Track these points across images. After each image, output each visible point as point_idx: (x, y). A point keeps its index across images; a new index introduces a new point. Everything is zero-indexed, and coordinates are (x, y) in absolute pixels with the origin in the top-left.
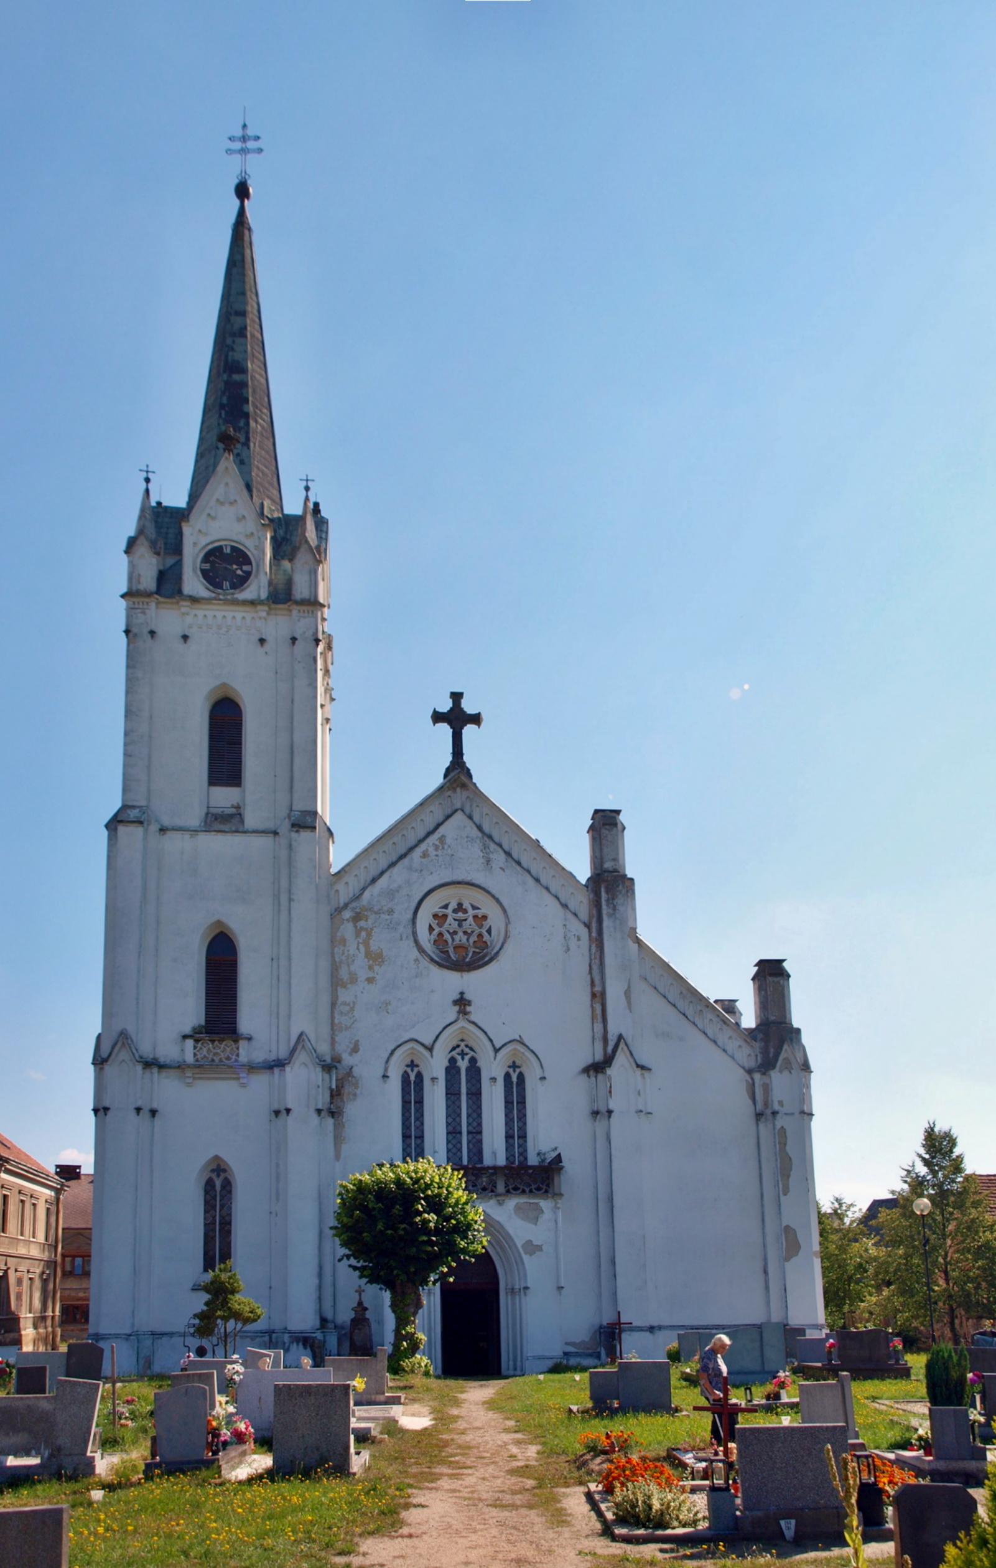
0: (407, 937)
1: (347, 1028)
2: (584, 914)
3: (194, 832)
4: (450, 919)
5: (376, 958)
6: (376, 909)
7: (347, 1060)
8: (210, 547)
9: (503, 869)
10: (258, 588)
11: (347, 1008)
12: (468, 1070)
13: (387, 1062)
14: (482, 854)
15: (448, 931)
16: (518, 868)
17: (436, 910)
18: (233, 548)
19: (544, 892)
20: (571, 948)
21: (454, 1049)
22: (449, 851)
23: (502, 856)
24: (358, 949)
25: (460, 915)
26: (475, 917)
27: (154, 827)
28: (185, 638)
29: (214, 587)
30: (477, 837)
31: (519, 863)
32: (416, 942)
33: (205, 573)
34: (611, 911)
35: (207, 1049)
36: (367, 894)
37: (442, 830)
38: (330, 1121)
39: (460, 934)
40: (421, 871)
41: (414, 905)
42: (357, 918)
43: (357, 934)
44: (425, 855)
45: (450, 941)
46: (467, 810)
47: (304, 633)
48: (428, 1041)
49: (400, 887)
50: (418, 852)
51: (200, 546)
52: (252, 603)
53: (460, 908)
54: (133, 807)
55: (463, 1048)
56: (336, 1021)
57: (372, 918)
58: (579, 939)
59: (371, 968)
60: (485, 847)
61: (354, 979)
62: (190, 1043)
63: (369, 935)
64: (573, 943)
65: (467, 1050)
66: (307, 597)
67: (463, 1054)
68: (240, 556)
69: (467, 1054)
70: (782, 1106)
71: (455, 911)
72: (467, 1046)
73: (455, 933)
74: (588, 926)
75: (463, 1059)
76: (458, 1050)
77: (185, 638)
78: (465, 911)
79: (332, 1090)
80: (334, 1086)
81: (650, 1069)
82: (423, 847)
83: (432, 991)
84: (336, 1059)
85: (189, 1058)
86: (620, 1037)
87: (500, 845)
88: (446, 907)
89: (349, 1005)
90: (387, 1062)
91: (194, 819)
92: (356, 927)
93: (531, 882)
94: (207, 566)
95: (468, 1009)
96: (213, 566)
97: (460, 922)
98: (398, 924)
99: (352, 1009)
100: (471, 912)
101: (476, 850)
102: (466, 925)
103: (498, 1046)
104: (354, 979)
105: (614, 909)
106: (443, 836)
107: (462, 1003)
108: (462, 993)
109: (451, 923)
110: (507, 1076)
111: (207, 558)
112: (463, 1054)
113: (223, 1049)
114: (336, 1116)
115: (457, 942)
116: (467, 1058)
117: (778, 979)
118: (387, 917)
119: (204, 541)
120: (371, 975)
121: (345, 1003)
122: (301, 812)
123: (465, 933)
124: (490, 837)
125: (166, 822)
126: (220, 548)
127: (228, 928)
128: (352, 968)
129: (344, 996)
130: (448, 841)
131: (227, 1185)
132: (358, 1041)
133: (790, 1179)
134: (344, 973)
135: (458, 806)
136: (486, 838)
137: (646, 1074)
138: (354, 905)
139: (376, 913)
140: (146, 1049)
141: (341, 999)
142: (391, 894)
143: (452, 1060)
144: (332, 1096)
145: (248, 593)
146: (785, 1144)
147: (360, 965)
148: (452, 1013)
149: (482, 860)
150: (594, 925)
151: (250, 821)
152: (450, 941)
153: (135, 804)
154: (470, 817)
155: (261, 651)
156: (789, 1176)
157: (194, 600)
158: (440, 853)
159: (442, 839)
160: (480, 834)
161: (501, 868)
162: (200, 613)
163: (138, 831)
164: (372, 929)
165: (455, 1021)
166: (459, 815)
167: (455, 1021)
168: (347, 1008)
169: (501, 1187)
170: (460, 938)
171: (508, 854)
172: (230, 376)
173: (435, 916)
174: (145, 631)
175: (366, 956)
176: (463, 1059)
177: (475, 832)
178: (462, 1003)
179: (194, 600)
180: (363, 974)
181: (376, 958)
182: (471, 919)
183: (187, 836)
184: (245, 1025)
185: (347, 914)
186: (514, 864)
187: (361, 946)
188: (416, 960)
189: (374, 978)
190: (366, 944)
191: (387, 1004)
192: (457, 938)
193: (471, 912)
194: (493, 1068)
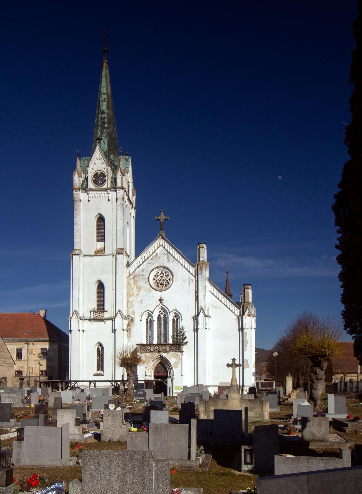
0: (147, 282)
1: (132, 307)
2: (194, 274)
3: (92, 256)
4: (159, 276)
6: (139, 275)
7: (131, 315)
8: (95, 173)
9: (172, 262)
10: (108, 184)
11: (131, 302)
12: (163, 317)
13: (141, 316)
14: (167, 258)
15: (158, 280)
16: (177, 261)
17: (155, 274)
18: (101, 173)
19: (184, 268)
20: (190, 284)
21: (160, 312)
22: (159, 258)
23: (173, 258)
24: (134, 286)
25: (162, 275)
26: (166, 276)
27: (82, 256)
28: (89, 201)
29: (96, 185)
30: (166, 253)
31: (177, 260)
32: (149, 283)
33: (94, 181)
34: (201, 273)
35: (96, 315)
36: (137, 271)
37: (156, 252)
38: (127, 332)
39: (162, 280)
40: (151, 264)
41: (149, 273)
42: (134, 278)
43: (134, 282)
44: (152, 259)
45: (159, 282)
46: (164, 246)
47: (120, 197)
48: (152, 311)
49: (145, 268)
50: (150, 258)
51: (92, 173)
52: (106, 190)
54: (77, 250)
56: (129, 306)
57: (138, 277)
58: (193, 281)
59: (137, 291)
60: (168, 256)
61: (133, 294)
62: (92, 313)
63: (137, 283)
64: (191, 282)
65: (163, 312)
66: (121, 186)
67: (162, 313)
68: (103, 175)
69: (163, 313)
70: (246, 326)
71: (160, 274)
72: (163, 311)
73: (160, 280)
74: (195, 277)
75: (162, 315)
76: (161, 312)
77: (89, 201)
78: (163, 274)
79: (127, 324)
80: (128, 323)
81: (210, 317)
82: (152, 256)
83: (154, 297)
84: (129, 316)
85: (92, 317)
86: (202, 308)
87: (172, 255)
88: (158, 273)
89: (132, 301)
90: (141, 316)
91: (93, 253)
92: (134, 280)
93: (180, 265)
94: (94, 179)
95: (163, 301)
96: (96, 179)
97: (161, 277)
98: (145, 279)
99: (133, 303)
100: (165, 274)
101: (166, 257)
102: (163, 278)
103: (170, 311)
104: (133, 294)
105: (202, 272)
106: (157, 253)
107: (161, 300)
108: (161, 297)
110: (173, 319)
111: (94, 177)
112: (162, 313)
113: (101, 314)
114: (128, 331)
115: (161, 283)
116: (163, 314)
117: (248, 290)
118: (142, 277)
119: (93, 171)
120: (138, 293)
121: (131, 301)
122: (119, 249)
123: (163, 280)
124: (169, 253)
125: (85, 254)
126: (97, 173)
127: (102, 282)
128: (133, 291)
129: (131, 299)
130: (158, 254)
131: (103, 349)
132: (134, 311)
133: (247, 346)
134: (131, 293)
135: (161, 244)
136: (168, 253)
137: (209, 318)
138: (133, 274)
139: (139, 276)
140: (81, 315)
141: (130, 300)
142: (143, 270)
143: (159, 315)
144: (127, 326)
145: (105, 187)
146: (246, 337)
147: (135, 291)
149: (167, 260)
150: (196, 277)
151: (107, 252)
152: (159, 282)
153: (77, 249)
154: (164, 248)
155: (109, 203)
156: (247, 346)
157: (91, 190)
158: (156, 258)
159: (157, 254)
160: (167, 252)
161: (172, 262)
163: (78, 256)
164: (138, 280)
165: (159, 305)
166: (161, 247)
167: (159, 305)
168: (131, 302)
169: (168, 350)
171: (174, 258)
172: (101, 115)
173: (155, 276)
174: (78, 200)
175: (136, 288)
176: (162, 315)
177: (165, 252)
178: (161, 300)
179: (91, 190)
180: (136, 293)
181: (139, 289)
182: (164, 276)
183: (91, 257)
184: (106, 308)
185: (131, 277)
186: (176, 260)
187: (135, 285)
188: (149, 289)
189: (138, 294)
190: (136, 284)
191: (142, 301)
192: (161, 281)
193: (165, 274)
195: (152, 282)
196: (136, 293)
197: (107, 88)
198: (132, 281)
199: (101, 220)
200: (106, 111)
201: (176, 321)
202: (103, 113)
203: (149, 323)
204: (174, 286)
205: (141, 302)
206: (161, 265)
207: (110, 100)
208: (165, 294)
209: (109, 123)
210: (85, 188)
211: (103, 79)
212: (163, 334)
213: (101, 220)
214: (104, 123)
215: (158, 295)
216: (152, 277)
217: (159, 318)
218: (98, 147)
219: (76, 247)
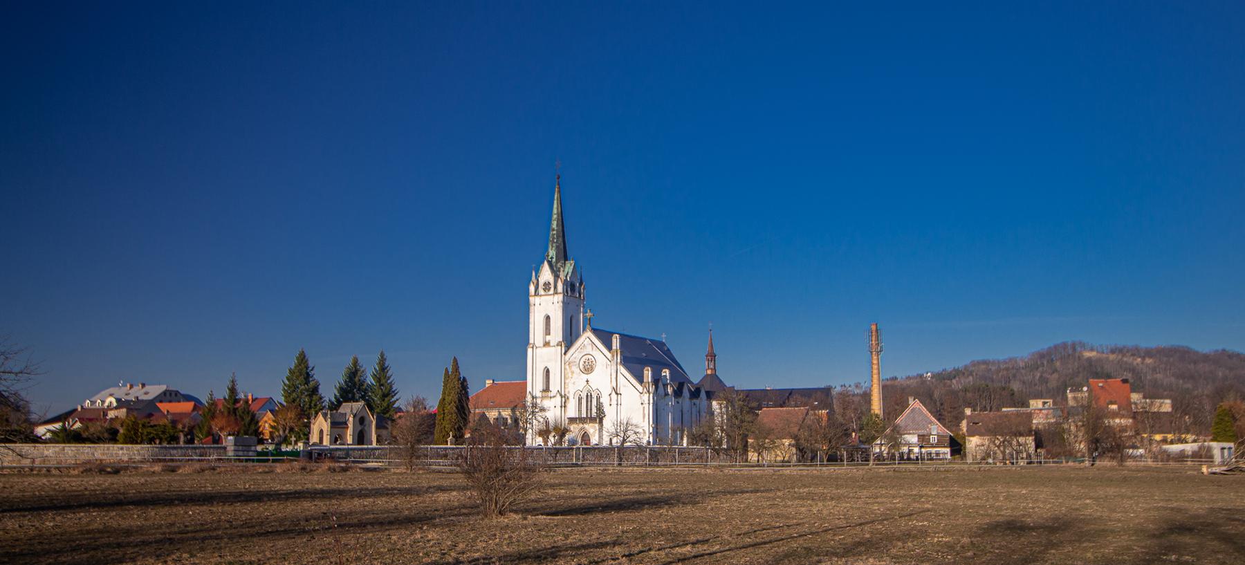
5: (573, 372)
7: (568, 395)
10: (552, 291)
52: (551, 295)
53: (588, 360)
55: (589, 391)
91: (542, 345)
101: (590, 346)
107: (587, 381)
109: (587, 363)
134: (567, 376)
142: (575, 358)
148: (586, 383)
151: (551, 344)
157: (541, 296)
162: (543, 298)
170: (588, 366)
177: (590, 342)
178: (587, 381)
180: (570, 376)
181: (573, 372)
184: (550, 389)
194: (594, 396)
195: (581, 367)
196: (570, 376)
197: (558, 209)
198: (567, 367)
199: (548, 318)
200: (556, 228)
201: (598, 399)
202: (553, 230)
203: (580, 400)
204: (597, 370)
205: (574, 383)
206: (588, 353)
207: (560, 218)
208: (589, 377)
209: (557, 238)
210: (536, 294)
211: (555, 202)
212: (589, 409)
213: (548, 318)
214: (553, 238)
215: (585, 377)
216: (582, 363)
217: (587, 396)
218: (546, 262)
219: (531, 341)
